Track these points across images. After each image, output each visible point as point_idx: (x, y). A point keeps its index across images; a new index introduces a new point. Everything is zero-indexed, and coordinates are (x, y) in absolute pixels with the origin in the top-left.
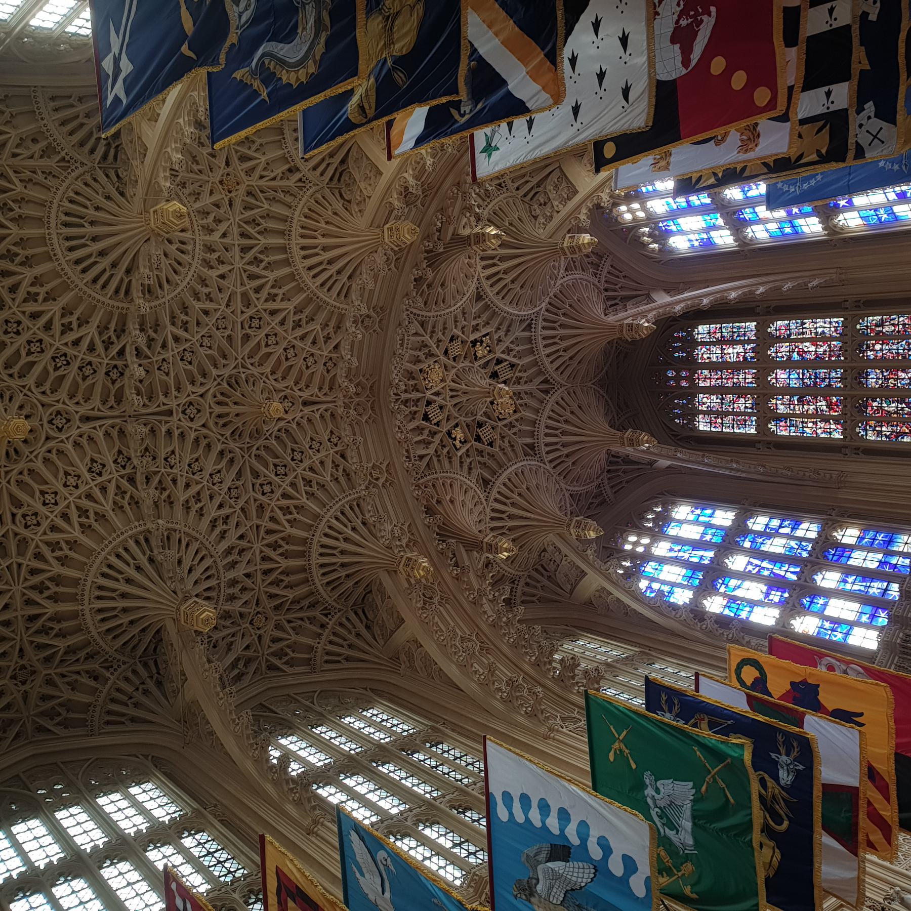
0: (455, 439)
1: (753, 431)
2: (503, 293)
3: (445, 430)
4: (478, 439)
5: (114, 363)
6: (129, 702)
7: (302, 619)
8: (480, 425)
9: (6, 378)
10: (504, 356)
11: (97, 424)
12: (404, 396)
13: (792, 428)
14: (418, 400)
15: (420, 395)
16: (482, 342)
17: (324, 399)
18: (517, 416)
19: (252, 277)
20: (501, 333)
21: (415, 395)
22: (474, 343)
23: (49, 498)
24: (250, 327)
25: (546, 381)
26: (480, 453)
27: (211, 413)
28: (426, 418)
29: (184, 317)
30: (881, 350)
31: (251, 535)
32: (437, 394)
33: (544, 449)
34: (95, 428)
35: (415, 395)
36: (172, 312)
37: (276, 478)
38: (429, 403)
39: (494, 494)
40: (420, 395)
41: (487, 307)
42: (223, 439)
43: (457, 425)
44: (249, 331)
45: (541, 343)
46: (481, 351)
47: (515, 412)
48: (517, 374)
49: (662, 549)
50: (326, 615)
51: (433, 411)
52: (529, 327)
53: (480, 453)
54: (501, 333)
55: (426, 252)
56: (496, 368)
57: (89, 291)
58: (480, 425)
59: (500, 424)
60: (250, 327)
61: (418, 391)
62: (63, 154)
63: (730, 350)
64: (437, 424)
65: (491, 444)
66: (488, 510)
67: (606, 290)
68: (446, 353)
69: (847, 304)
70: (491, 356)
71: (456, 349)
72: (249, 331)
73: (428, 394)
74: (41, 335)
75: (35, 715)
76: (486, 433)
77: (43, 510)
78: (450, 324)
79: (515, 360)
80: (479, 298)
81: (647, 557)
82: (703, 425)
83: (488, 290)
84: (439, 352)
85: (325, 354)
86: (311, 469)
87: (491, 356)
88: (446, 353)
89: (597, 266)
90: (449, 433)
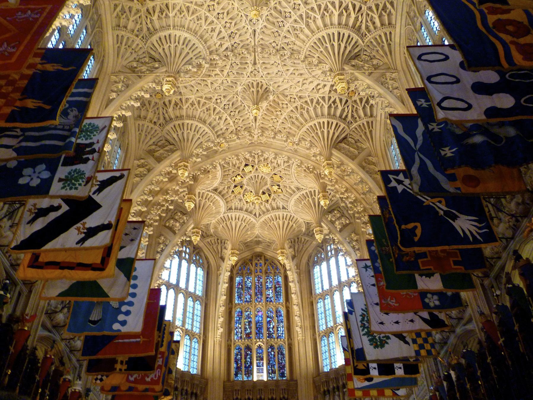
0: (236, 177)
1: (236, 302)
2: (299, 200)
3: (240, 173)
4: (235, 186)
5: (279, 45)
6: (127, 46)
7: (159, 114)
8: (241, 187)
9: (275, 2)
10: (272, 197)
11: (252, 36)
12: (256, 156)
13: (238, 319)
14: (254, 162)
15: (256, 162)
16: (279, 189)
17: (257, 124)
18: (245, 203)
19: (312, 101)
20: (282, 197)
21: (256, 161)
22: (279, 185)
23: (221, 16)
24: (291, 98)
25: (260, 215)
26: (229, 188)
27: (254, 81)
28: (246, 165)
29: (297, 74)
30: (271, 354)
31: (199, 94)
32: (257, 169)
33: (229, 215)
34: (251, 35)
35: (256, 161)
36: (299, 70)
37: (223, 105)
38: (253, 166)
39: (210, 194)
40: (256, 162)
41: (294, 192)
42: (242, 84)
43: (242, 177)
44: (289, 97)
45: (277, 214)
46: (275, 188)
47: (247, 202)
48: (264, 203)
49: (184, 263)
50: (160, 125)
51: (249, 168)
52: (284, 208)
53: (229, 188)
54: (282, 197)
55: (320, 174)
56: (267, 194)
57: (311, 41)
58: (241, 187)
59: (242, 196)
60: (291, 98)
61: (259, 162)
62: (368, 35)
63: (271, 291)
64: (243, 169)
65: (233, 191)
66: (203, 191)
67: (298, 238)
68: (275, 174)
69: (290, 340)
70: (272, 192)
71: (277, 178)
72: (289, 97)
73: (256, 166)
74: (293, 18)
75: (123, 6)
76: (238, 189)
77: (215, 14)
78: (288, 177)
79: (269, 202)
80: (298, 189)
81: (181, 259)
82: (238, 279)
83: (301, 193)
84: (275, 172)
85: (278, 127)
86: (226, 119)
87: (272, 192)
88: (275, 174)
89: (308, 235)
90: (239, 175)
